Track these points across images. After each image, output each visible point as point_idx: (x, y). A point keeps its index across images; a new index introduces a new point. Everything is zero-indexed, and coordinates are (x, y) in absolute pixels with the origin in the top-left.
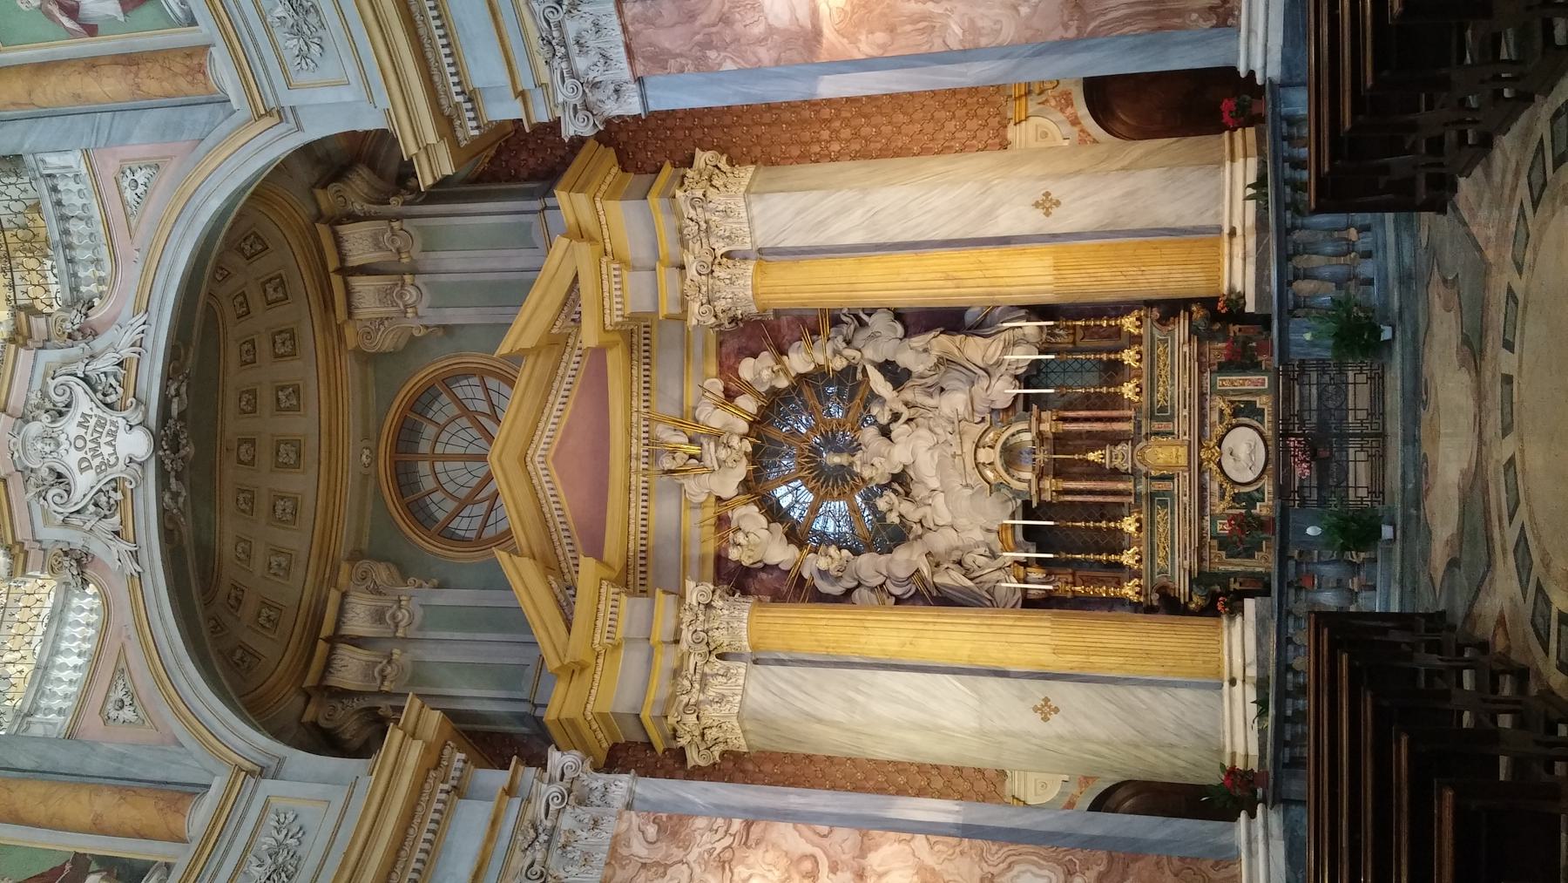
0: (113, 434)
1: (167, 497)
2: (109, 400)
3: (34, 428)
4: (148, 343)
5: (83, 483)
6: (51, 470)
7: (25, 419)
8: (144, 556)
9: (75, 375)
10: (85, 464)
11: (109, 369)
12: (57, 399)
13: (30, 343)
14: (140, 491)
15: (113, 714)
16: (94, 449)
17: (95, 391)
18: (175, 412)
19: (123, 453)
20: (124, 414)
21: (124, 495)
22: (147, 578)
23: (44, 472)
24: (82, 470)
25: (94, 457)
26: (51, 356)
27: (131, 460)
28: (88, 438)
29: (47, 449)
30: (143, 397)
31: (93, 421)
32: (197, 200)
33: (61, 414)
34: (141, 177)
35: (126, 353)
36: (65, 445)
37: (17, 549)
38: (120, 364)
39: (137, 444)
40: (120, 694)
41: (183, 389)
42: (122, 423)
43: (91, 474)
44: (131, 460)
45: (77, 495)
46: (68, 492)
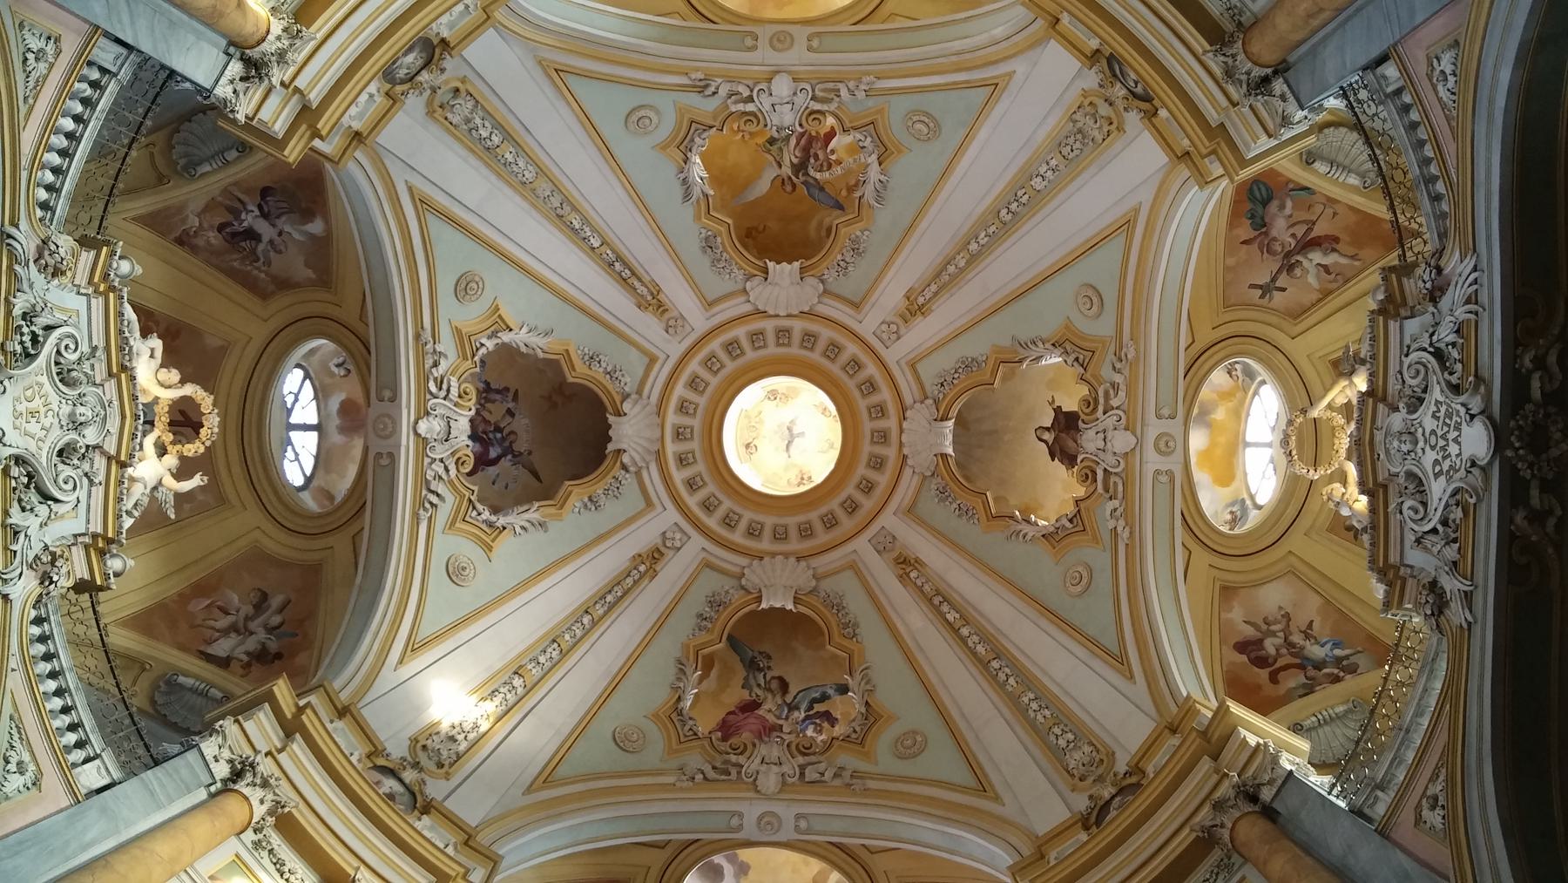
0: (1458, 428)
1: (1519, 518)
2: (1454, 379)
3: (1397, 420)
4: (1484, 297)
5: (1438, 490)
6: (1410, 475)
7: (1397, 409)
8: (1478, 599)
9: (1425, 350)
10: (1438, 469)
11: (1452, 338)
12: (1414, 382)
13: (1403, 312)
14: (1484, 505)
15: (1426, 813)
16: (1443, 449)
17: (1444, 368)
18: (1536, 394)
19: (1465, 456)
20: (1462, 399)
21: (1465, 512)
22: (1477, 629)
23: (1401, 480)
24: (1437, 476)
25: (1444, 458)
26: (1412, 326)
27: (1473, 464)
28: (1440, 433)
29: (1405, 448)
30: (1485, 373)
31: (1443, 409)
32: (1487, 73)
33: (1421, 400)
34: (1446, 64)
35: (1461, 313)
36: (1421, 444)
37: (1391, 575)
38: (1457, 332)
39: (1476, 441)
40: (1437, 788)
41: (1552, 359)
42: (1462, 410)
43: (1442, 479)
44: (1473, 464)
45: (1431, 508)
46: (1424, 504)
